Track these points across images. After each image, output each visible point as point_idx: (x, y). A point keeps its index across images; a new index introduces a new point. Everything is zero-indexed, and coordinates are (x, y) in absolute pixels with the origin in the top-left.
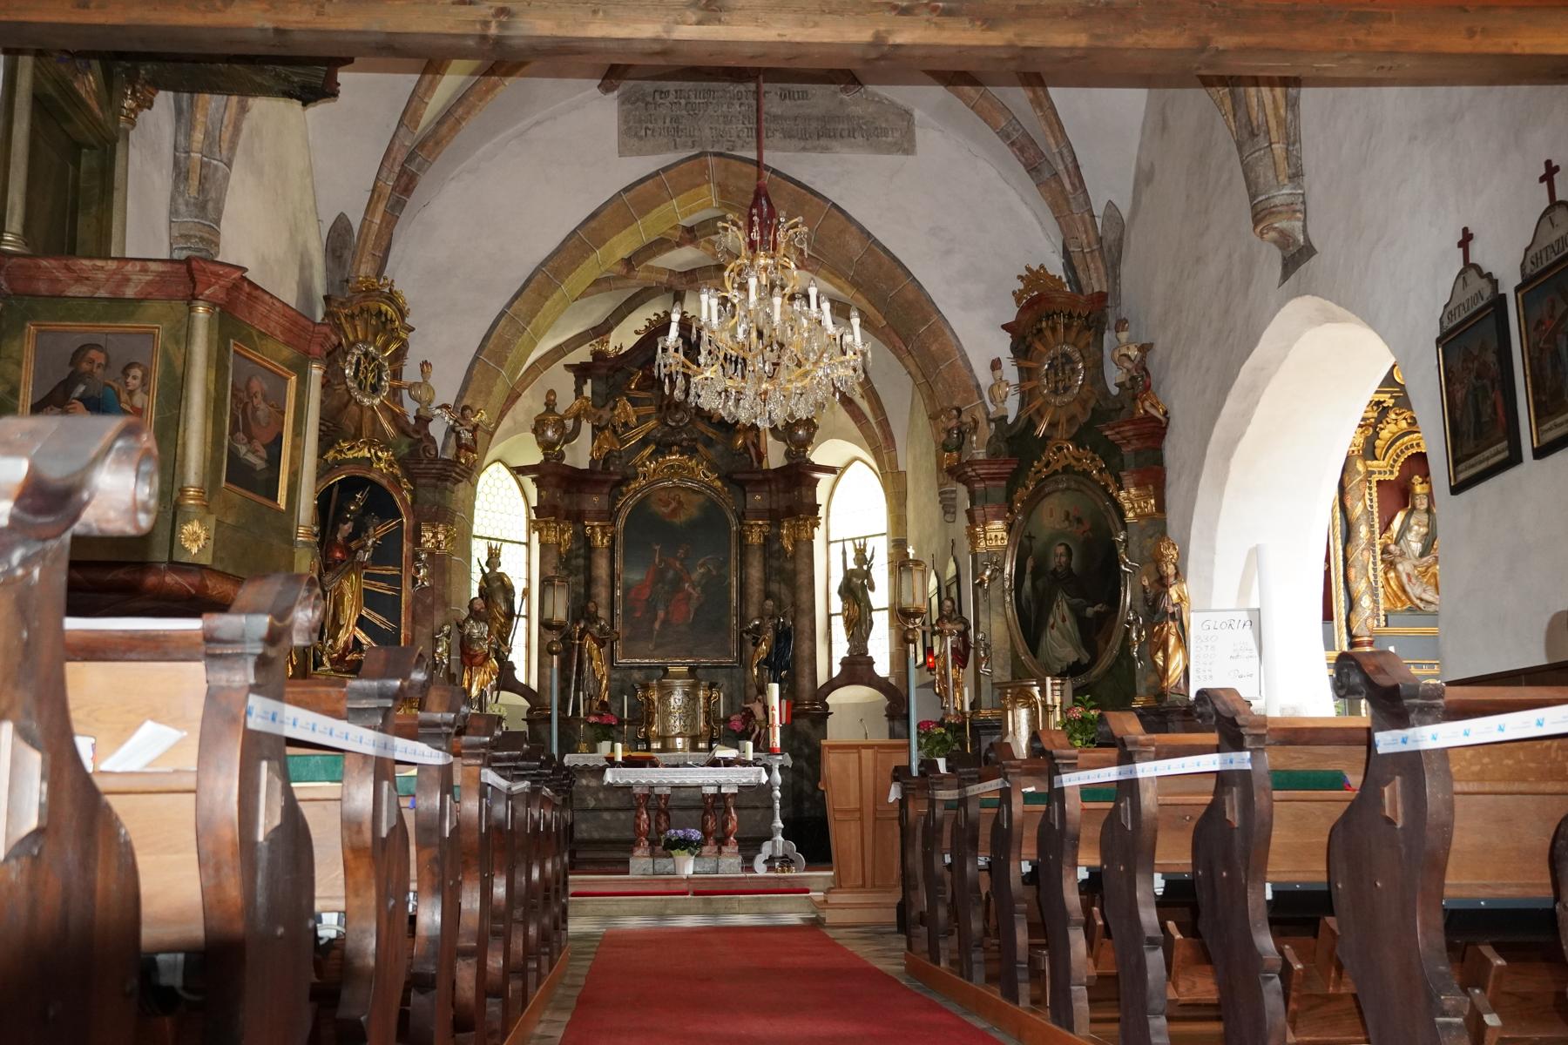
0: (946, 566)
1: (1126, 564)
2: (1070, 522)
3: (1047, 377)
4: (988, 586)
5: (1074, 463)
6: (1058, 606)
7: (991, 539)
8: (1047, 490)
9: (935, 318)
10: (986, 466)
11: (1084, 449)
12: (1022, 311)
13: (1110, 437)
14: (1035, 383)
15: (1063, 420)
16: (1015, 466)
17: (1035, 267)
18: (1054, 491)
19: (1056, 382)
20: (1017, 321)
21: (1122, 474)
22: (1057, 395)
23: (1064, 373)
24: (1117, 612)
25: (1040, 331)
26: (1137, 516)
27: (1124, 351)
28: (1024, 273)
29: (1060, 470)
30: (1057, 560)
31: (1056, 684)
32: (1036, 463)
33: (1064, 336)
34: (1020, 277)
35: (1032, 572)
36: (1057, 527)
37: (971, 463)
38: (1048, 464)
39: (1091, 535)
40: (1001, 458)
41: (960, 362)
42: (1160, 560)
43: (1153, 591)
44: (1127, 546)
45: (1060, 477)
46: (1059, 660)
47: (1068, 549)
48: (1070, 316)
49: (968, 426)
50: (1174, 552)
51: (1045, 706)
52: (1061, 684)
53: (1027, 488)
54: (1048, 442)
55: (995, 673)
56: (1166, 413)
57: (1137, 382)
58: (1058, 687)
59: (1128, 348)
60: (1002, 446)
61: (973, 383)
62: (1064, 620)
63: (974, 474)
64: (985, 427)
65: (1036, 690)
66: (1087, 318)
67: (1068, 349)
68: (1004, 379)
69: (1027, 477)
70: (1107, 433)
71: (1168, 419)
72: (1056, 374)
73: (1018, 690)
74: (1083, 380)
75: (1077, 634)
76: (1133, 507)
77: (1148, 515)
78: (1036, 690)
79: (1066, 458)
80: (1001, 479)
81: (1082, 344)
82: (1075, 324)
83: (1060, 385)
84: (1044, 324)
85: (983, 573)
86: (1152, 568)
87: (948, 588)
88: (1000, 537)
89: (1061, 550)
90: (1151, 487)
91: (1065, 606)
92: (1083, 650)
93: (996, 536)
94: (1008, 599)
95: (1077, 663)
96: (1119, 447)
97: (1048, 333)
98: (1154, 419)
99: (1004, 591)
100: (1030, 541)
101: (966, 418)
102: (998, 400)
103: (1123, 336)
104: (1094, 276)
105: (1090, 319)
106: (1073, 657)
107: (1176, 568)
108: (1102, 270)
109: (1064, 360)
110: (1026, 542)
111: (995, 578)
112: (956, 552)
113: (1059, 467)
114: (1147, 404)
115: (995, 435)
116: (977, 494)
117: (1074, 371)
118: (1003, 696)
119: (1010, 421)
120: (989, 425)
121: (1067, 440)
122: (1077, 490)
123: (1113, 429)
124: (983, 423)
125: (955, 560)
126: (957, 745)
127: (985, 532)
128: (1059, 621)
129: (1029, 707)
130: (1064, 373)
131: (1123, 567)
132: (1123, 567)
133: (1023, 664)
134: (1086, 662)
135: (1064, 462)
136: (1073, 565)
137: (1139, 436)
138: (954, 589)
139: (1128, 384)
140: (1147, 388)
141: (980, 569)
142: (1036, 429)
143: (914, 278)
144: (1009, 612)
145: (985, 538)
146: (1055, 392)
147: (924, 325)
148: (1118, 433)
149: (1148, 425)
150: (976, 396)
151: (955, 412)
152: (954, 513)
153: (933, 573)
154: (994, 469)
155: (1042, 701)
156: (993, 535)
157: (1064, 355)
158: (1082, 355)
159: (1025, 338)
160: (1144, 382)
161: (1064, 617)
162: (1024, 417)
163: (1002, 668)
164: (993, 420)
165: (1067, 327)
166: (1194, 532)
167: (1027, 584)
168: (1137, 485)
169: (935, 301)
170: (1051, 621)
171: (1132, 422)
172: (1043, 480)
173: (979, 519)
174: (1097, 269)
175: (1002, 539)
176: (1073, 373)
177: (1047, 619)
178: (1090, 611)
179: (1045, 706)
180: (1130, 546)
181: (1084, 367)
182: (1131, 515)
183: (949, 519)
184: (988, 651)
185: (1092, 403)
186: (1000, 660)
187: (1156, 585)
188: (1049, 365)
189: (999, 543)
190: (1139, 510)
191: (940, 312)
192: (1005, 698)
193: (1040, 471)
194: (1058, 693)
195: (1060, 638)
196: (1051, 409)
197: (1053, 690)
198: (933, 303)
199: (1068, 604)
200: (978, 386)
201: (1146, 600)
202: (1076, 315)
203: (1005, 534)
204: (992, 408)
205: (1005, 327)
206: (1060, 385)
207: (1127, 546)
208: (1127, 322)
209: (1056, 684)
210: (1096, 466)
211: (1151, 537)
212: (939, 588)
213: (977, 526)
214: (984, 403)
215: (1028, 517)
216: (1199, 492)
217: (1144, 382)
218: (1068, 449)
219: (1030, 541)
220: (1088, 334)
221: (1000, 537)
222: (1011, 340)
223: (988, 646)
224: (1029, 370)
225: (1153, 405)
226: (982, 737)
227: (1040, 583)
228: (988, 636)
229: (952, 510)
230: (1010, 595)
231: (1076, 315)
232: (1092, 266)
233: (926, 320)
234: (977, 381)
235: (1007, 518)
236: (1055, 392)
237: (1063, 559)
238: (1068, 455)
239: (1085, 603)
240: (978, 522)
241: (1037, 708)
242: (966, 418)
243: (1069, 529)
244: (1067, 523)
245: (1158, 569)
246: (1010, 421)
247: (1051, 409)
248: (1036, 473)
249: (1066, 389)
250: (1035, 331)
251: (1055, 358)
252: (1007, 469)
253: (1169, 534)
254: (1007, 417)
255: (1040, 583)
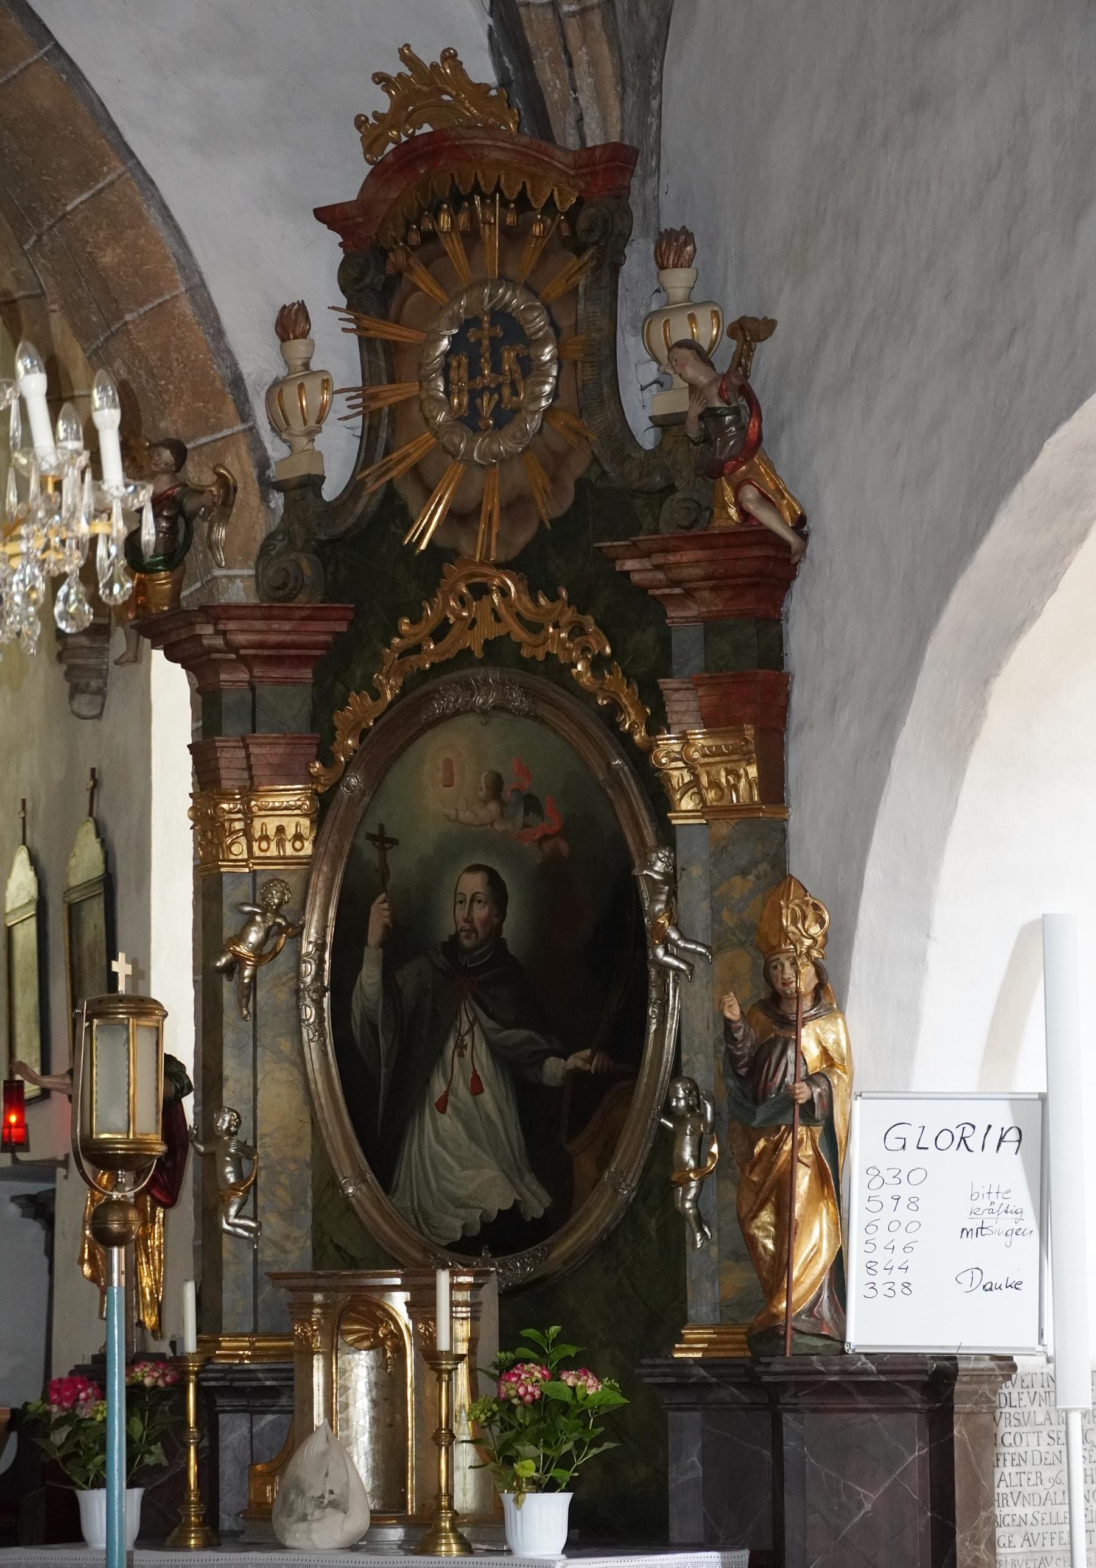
0: (68, 845)
1: (666, 941)
2: (502, 803)
3: (446, 371)
4: (253, 977)
5: (519, 633)
6: (460, 1047)
7: (265, 838)
8: (437, 708)
9: (114, 171)
10: (259, 625)
11: (554, 597)
12: (380, 174)
13: (636, 578)
14: (411, 388)
15: (493, 505)
16: (342, 627)
17: (429, 56)
18: (457, 713)
19: (475, 395)
20: (365, 202)
21: (665, 683)
22: (476, 430)
23: (496, 368)
24: (635, 1075)
25: (430, 237)
26: (705, 809)
27: (681, 330)
28: (395, 68)
29: (478, 654)
30: (462, 912)
31: (460, 1286)
32: (405, 625)
33: (501, 264)
34: (380, 79)
35: (384, 944)
36: (466, 816)
37: (215, 613)
38: (440, 632)
39: (564, 847)
40: (301, 600)
41: (186, 307)
42: (775, 950)
43: (753, 1035)
44: (673, 894)
45: (479, 673)
46: (461, 1204)
47: (495, 883)
48: (523, 203)
49: (205, 499)
50: (815, 930)
51: (429, 1355)
52: (474, 1287)
53: (376, 695)
54: (446, 567)
55: (267, 1231)
56: (800, 524)
57: (722, 429)
58: (463, 1296)
59: (692, 318)
60: (305, 564)
61: (219, 371)
62: (476, 1088)
63: (219, 642)
64: (254, 500)
65: (398, 1302)
66: (572, 216)
67: (514, 300)
68: (314, 366)
69: (377, 660)
70: (629, 565)
71: (804, 537)
72: (474, 371)
73: (343, 1298)
74: (555, 394)
75: (515, 1133)
76: (696, 782)
77: (738, 809)
78: (398, 1302)
79: (498, 619)
80: (301, 661)
81: (555, 289)
82: (537, 230)
83: (486, 404)
84: (445, 221)
85: (241, 938)
86: (744, 961)
87: (73, 912)
88: (290, 832)
89: (474, 883)
90: (749, 731)
91: (482, 1050)
92: (529, 1178)
93: (280, 830)
94: (310, 1013)
95: (511, 1217)
96: (659, 603)
97: (454, 247)
98: (766, 536)
99: (297, 992)
100: (383, 851)
101: (198, 473)
102: (297, 426)
103: (678, 280)
104: (585, 83)
105: (582, 224)
106: (499, 1199)
107: (819, 972)
108: (608, 69)
109: (499, 331)
110: (370, 852)
111: (275, 953)
112: (103, 808)
113: (475, 642)
114: (750, 494)
115: (285, 529)
116: (227, 700)
117: (529, 367)
118: (301, 1310)
119: (330, 491)
120: (265, 499)
121: (498, 566)
122: (527, 716)
123: (648, 555)
124: (248, 495)
125: (100, 832)
126: (157, 1448)
127: (248, 816)
128: (462, 1090)
129: (377, 1345)
130: (496, 368)
131: (660, 952)
132: (660, 952)
133: (349, 1207)
134: (539, 1213)
135: (488, 630)
136: (509, 929)
137: (719, 581)
138: (94, 916)
139: (693, 429)
140: (752, 447)
141: (229, 926)
142: (408, 524)
143: (57, 45)
144: (312, 1052)
145: (247, 832)
146: (470, 420)
147: (82, 189)
148: (658, 567)
149: (748, 553)
150: (231, 409)
151: (167, 455)
152: (101, 692)
153: (22, 857)
154: (281, 631)
155: (416, 1334)
156: (272, 825)
157: (501, 315)
158: (552, 323)
159: (384, 253)
160: (742, 428)
161: (476, 1078)
162: (374, 486)
163: (287, 1215)
164: (280, 486)
165: (512, 236)
166: (873, 873)
167: (370, 976)
168: (711, 722)
169: (118, 120)
170: (438, 1086)
171: (704, 541)
172: (423, 676)
173: (231, 779)
174: (594, 63)
175: (298, 837)
176: (526, 373)
177: (427, 1081)
178: (554, 1069)
179: (429, 1355)
180: (683, 895)
181: (558, 359)
182: (687, 803)
183: (86, 711)
184: (245, 1164)
185: (578, 466)
186: (281, 1193)
187: (762, 1017)
188: (454, 340)
189: (289, 851)
190: (711, 795)
191: (132, 154)
192: (306, 1321)
193: (417, 649)
194: (463, 1312)
195: (463, 1137)
196: (456, 471)
197: (453, 1304)
198: (113, 126)
199: (494, 1049)
200: (237, 382)
201: (732, 1060)
202: (538, 204)
203: (306, 822)
204: (275, 449)
205: (326, 215)
206: (486, 404)
207: (673, 894)
208: (689, 237)
209: (460, 1286)
210: (585, 650)
211: (744, 873)
212: (41, 905)
213: (228, 796)
214: (252, 432)
215: (376, 781)
216: (895, 763)
217: (742, 428)
218: (504, 592)
219: (383, 851)
220: (573, 262)
221: (290, 832)
222: (340, 255)
223: (247, 1151)
224: (392, 349)
225: (765, 498)
226: (223, 1419)
227: (408, 978)
228: (247, 1123)
229: (94, 684)
230: (318, 1004)
231: (538, 204)
232: (581, 55)
233: (87, 174)
234: (235, 365)
235: (313, 779)
236: (470, 420)
237: (480, 912)
238: (503, 611)
239: (544, 1045)
240: (226, 784)
241: (400, 1350)
242: (198, 473)
243: (499, 827)
244: (493, 807)
245: (768, 973)
246: (330, 491)
247: (456, 471)
248: (404, 653)
249: (504, 417)
250: (415, 238)
251: (468, 324)
252: (320, 632)
253: (795, 868)
254: (322, 479)
255: (408, 978)
